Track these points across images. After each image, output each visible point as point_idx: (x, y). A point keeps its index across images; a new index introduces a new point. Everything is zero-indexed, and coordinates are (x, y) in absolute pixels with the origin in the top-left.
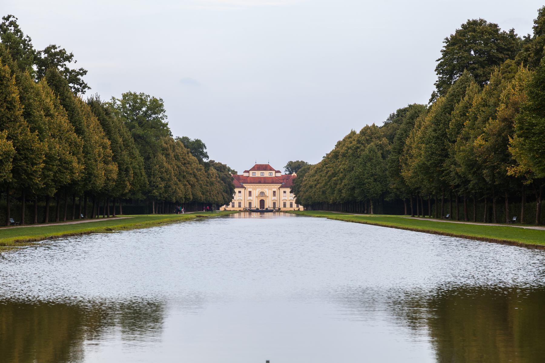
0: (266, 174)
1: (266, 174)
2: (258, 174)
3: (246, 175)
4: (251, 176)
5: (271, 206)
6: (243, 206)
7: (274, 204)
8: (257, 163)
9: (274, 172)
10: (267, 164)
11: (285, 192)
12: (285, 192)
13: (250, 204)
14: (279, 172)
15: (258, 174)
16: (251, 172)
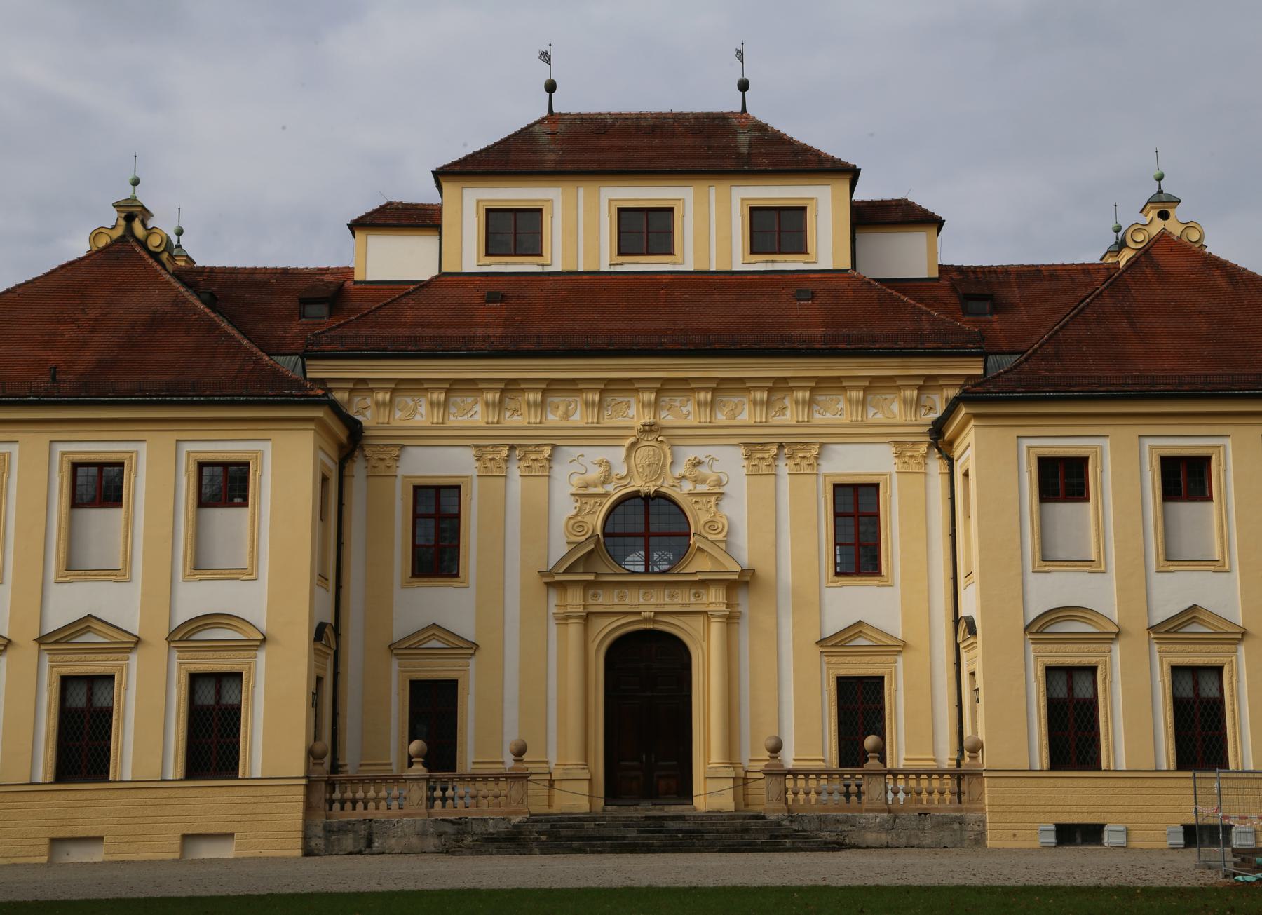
0: (711, 228)
1: (711, 228)
2: (579, 229)
3: (400, 260)
4: (466, 251)
5: (809, 736)
6: (273, 734)
7: (860, 705)
8: (565, 104)
9: (826, 208)
10: (728, 103)
11: (1063, 480)
12: (1063, 480)
13: (434, 709)
14: (904, 216)
15: (579, 229)
16: (468, 207)
